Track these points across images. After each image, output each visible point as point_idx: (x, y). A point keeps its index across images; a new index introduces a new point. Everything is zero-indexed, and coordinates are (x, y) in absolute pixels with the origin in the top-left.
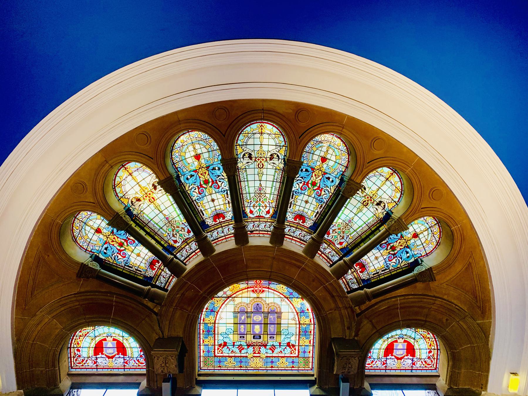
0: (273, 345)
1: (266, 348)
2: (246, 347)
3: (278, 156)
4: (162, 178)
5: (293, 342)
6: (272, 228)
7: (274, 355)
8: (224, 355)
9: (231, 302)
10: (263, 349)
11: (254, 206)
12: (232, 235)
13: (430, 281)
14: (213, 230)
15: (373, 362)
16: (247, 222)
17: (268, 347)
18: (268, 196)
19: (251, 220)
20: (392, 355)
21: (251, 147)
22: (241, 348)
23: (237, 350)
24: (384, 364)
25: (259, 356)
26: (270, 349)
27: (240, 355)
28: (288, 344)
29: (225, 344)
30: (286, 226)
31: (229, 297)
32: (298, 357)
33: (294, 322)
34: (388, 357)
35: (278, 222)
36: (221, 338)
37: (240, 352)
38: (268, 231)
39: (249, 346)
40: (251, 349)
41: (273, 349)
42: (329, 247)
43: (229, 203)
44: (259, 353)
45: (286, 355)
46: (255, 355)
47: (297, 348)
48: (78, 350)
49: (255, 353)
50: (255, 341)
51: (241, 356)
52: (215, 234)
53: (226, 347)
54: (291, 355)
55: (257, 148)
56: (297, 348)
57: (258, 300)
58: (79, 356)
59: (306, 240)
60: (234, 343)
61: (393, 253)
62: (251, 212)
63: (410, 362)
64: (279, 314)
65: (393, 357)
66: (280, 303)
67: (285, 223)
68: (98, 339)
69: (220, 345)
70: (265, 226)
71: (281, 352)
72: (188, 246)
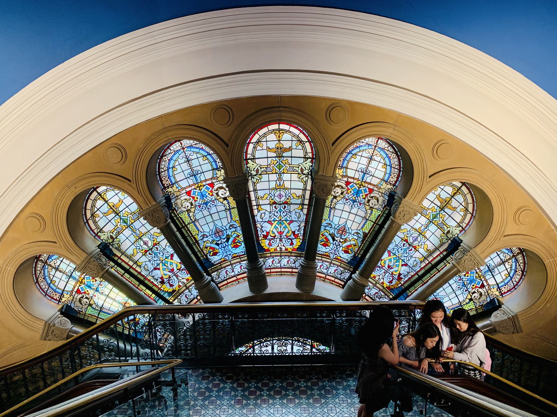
4: (145, 207)
6: (297, 264)
12: (245, 275)
13: (513, 333)
14: (220, 269)
16: (265, 257)
19: (269, 255)
30: (317, 261)
35: (306, 258)
38: (292, 268)
42: (375, 287)
52: (223, 273)
59: (344, 278)
67: (317, 258)
70: (288, 262)
72: (187, 291)
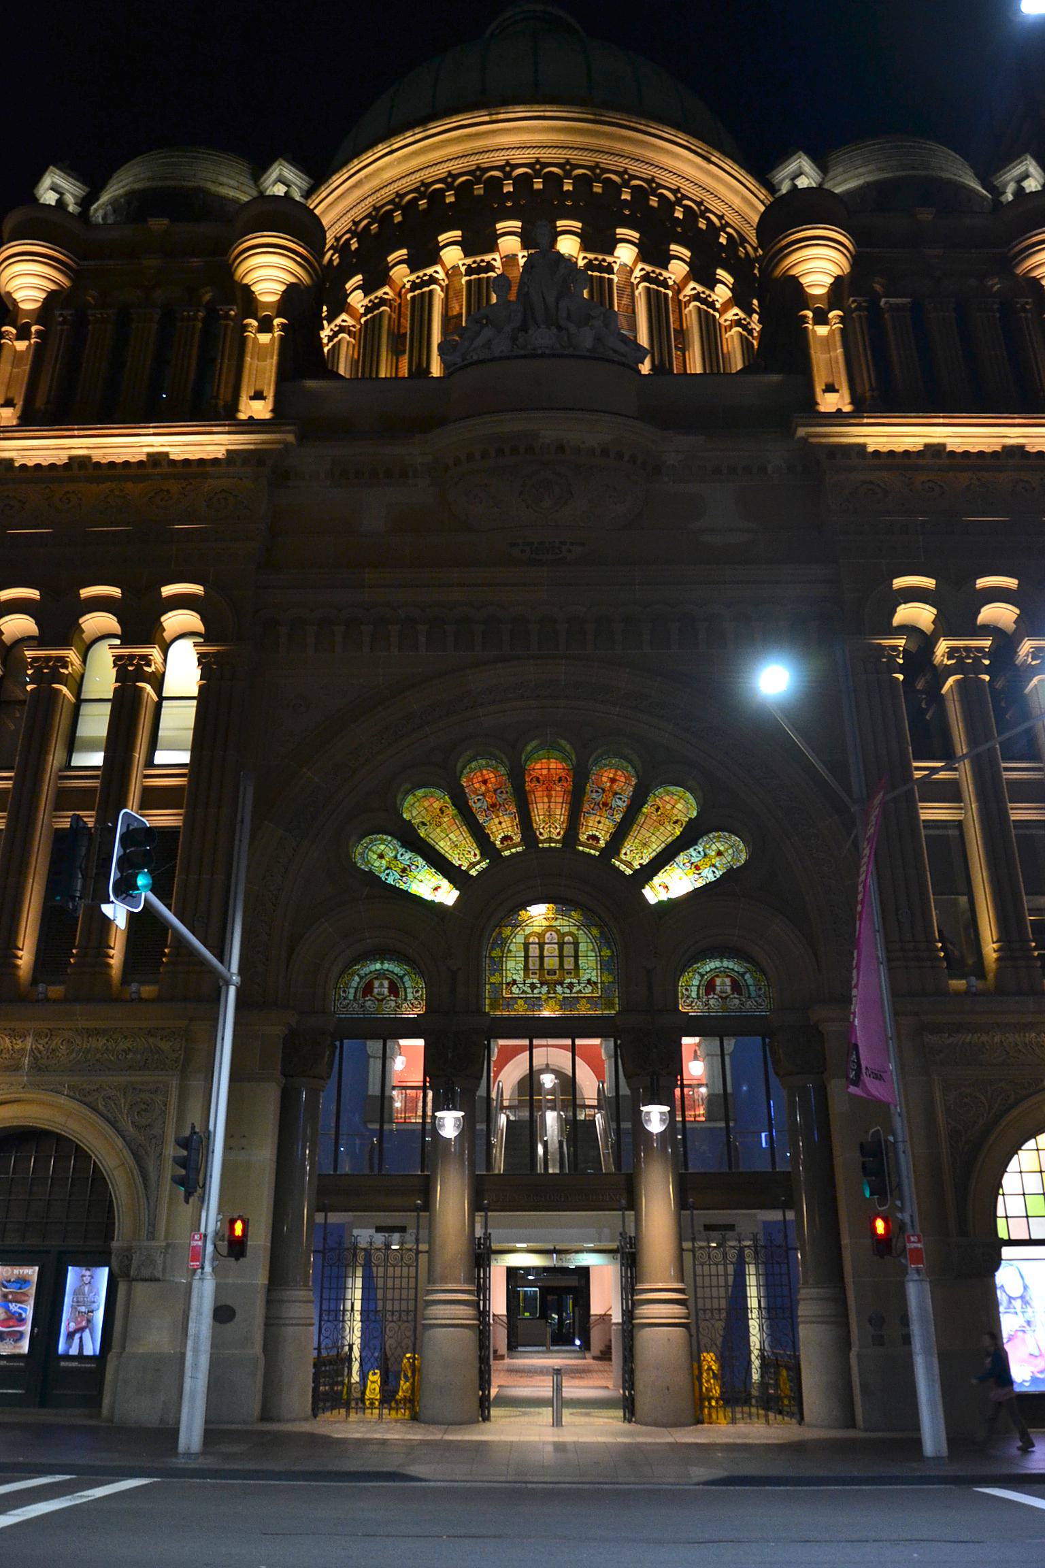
0: (571, 983)
1: (562, 987)
2: (539, 986)
3: (566, 778)
5: (594, 979)
7: (572, 995)
8: (514, 996)
9: (521, 932)
10: (559, 989)
11: (543, 828)
15: (692, 1002)
17: (565, 986)
18: (558, 817)
20: (714, 994)
21: (539, 772)
22: (533, 986)
23: (529, 990)
24: (706, 1005)
25: (555, 997)
26: (568, 987)
27: (532, 996)
28: (589, 981)
29: (514, 982)
31: (518, 926)
32: (601, 997)
33: (594, 954)
34: (710, 997)
36: (509, 974)
37: (532, 991)
39: (542, 984)
40: (545, 989)
41: (571, 986)
43: (517, 825)
44: (554, 993)
45: (587, 995)
46: (550, 995)
47: (599, 985)
48: (344, 991)
49: (550, 993)
50: (548, 978)
51: (534, 997)
53: (515, 986)
54: (593, 995)
55: (545, 772)
56: (599, 985)
57: (551, 928)
58: (345, 999)
60: (524, 981)
61: (697, 872)
62: (541, 834)
63: (737, 1002)
64: (576, 944)
65: (716, 997)
66: (576, 932)
68: (368, 978)
69: (508, 984)
71: (580, 990)
